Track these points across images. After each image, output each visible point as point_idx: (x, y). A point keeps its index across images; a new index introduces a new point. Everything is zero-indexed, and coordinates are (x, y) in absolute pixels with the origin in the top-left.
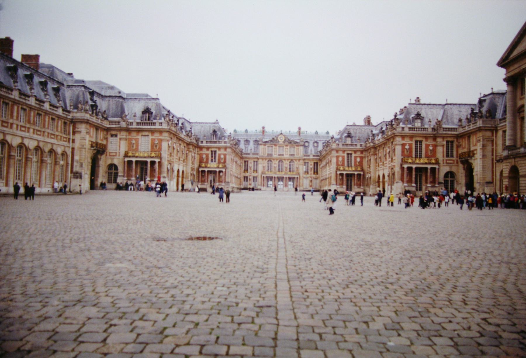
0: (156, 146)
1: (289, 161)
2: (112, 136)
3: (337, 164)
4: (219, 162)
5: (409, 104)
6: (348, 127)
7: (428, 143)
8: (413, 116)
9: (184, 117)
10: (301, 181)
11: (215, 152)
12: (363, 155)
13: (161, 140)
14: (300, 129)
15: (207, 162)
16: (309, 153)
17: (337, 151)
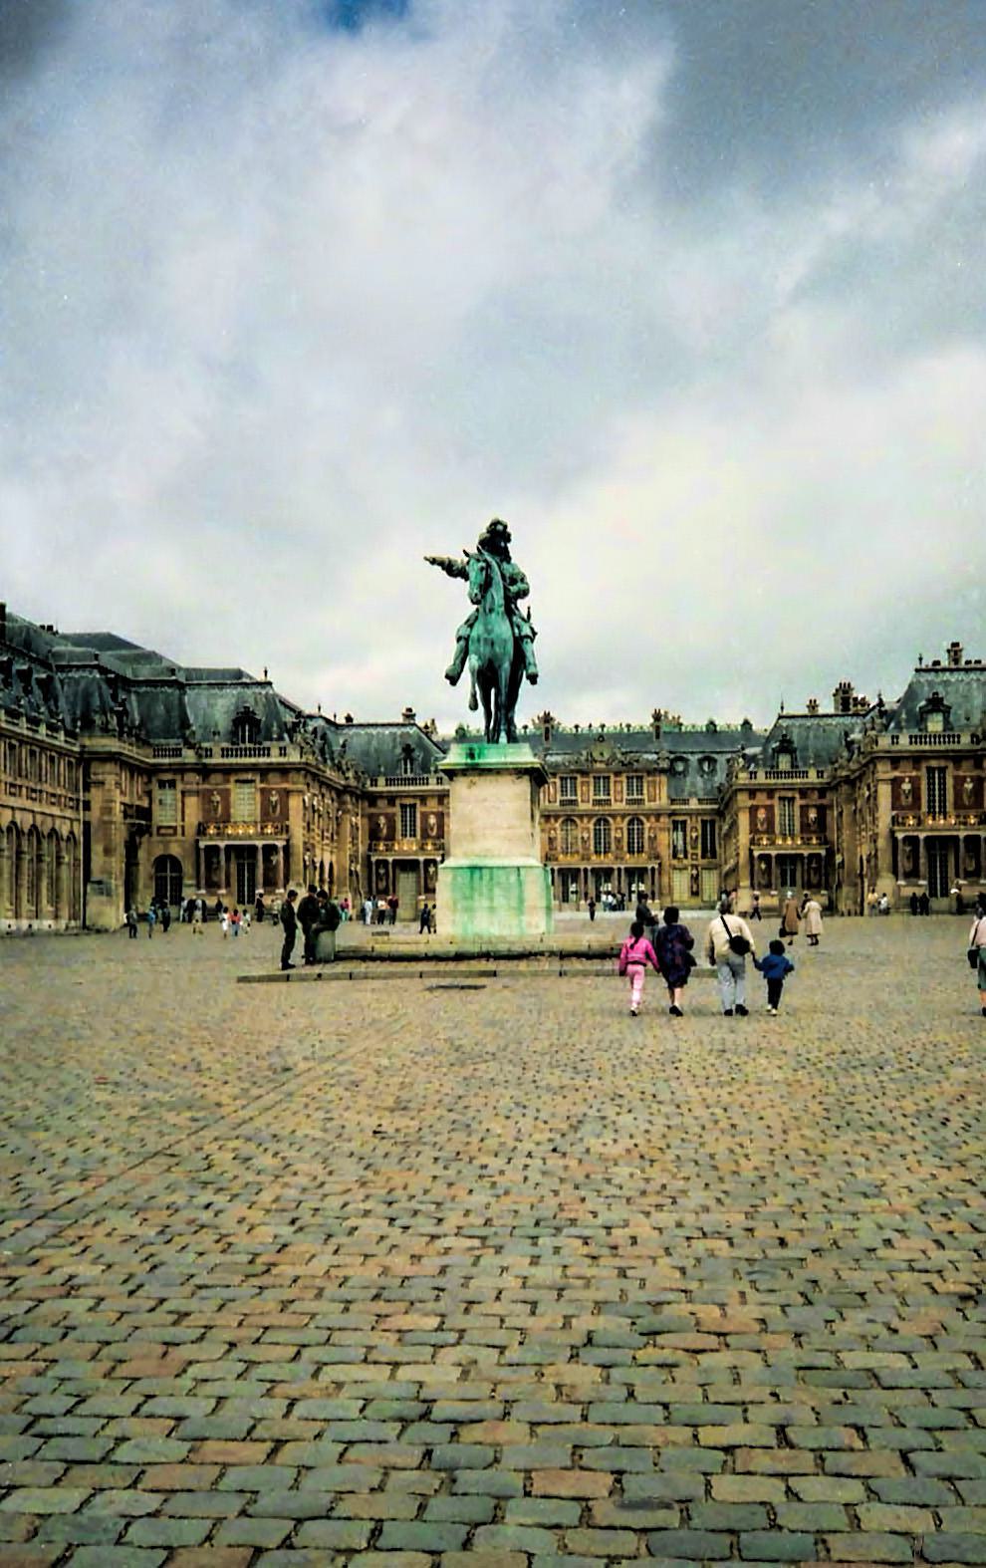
0: (275, 808)
1: (627, 819)
2: (162, 785)
3: (754, 830)
4: (425, 835)
5: (917, 670)
6: (784, 723)
7: (961, 773)
8: (923, 703)
9: (323, 714)
10: (665, 880)
11: (413, 806)
12: (825, 802)
13: (288, 793)
14: (657, 717)
15: (391, 837)
16: (685, 795)
17: (753, 793)
